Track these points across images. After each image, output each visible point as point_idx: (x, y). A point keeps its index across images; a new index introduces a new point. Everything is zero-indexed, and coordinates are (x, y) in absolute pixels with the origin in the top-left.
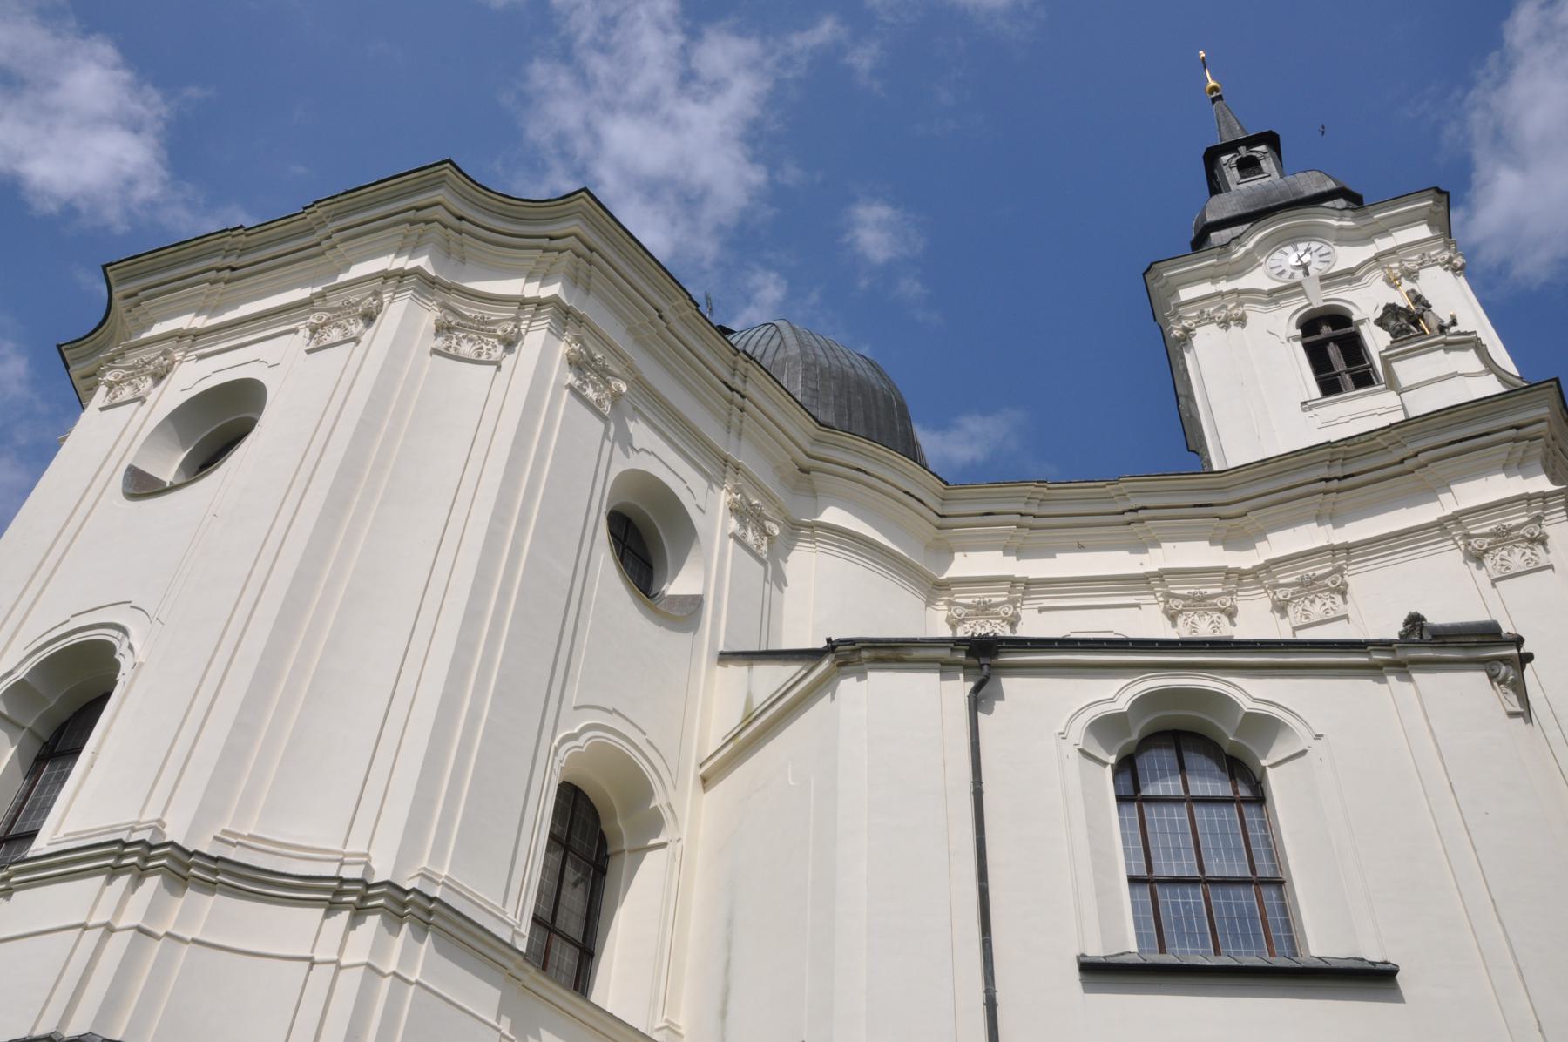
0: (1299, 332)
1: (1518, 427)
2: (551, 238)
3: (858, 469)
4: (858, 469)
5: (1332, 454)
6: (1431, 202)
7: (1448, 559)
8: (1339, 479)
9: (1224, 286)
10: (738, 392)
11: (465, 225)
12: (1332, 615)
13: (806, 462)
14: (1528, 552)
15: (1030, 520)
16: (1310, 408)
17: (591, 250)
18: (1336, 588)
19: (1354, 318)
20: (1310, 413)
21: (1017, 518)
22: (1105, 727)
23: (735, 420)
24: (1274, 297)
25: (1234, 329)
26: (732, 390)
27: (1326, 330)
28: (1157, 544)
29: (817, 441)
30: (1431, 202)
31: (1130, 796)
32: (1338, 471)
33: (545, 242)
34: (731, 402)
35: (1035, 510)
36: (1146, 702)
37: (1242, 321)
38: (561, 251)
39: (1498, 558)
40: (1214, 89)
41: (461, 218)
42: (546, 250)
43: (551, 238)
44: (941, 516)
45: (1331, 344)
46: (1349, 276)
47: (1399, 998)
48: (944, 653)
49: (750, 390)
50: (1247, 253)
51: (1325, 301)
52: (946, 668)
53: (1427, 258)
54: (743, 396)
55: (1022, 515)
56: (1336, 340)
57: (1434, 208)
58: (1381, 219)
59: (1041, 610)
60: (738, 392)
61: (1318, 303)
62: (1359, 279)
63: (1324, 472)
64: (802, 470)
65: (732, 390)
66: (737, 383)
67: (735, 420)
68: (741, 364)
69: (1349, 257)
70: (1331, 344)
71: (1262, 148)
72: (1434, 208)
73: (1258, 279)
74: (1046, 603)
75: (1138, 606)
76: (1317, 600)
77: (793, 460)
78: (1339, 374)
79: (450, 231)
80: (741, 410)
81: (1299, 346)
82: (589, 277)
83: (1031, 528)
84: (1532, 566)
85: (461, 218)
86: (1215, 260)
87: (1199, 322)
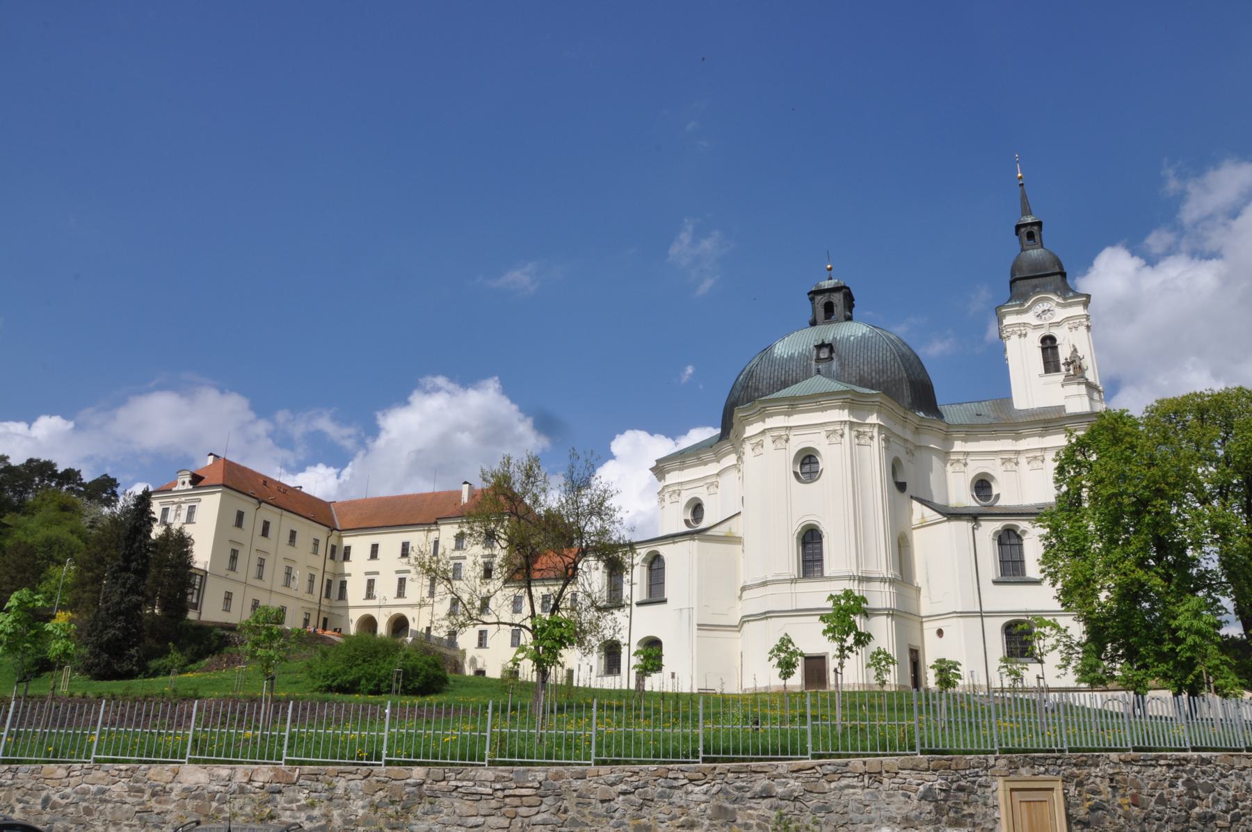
19: (1057, 343)
24: (1036, 327)
25: (1022, 338)
27: (1048, 342)
29: (920, 421)
31: (1000, 544)
36: (1004, 527)
37: (1025, 335)
40: (1021, 178)
46: (1058, 324)
49: (909, 417)
52: (968, 520)
61: (1047, 334)
64: (917, 428)
69: (1061, 314)
71: (1036, 228)
73: (1030, 318)
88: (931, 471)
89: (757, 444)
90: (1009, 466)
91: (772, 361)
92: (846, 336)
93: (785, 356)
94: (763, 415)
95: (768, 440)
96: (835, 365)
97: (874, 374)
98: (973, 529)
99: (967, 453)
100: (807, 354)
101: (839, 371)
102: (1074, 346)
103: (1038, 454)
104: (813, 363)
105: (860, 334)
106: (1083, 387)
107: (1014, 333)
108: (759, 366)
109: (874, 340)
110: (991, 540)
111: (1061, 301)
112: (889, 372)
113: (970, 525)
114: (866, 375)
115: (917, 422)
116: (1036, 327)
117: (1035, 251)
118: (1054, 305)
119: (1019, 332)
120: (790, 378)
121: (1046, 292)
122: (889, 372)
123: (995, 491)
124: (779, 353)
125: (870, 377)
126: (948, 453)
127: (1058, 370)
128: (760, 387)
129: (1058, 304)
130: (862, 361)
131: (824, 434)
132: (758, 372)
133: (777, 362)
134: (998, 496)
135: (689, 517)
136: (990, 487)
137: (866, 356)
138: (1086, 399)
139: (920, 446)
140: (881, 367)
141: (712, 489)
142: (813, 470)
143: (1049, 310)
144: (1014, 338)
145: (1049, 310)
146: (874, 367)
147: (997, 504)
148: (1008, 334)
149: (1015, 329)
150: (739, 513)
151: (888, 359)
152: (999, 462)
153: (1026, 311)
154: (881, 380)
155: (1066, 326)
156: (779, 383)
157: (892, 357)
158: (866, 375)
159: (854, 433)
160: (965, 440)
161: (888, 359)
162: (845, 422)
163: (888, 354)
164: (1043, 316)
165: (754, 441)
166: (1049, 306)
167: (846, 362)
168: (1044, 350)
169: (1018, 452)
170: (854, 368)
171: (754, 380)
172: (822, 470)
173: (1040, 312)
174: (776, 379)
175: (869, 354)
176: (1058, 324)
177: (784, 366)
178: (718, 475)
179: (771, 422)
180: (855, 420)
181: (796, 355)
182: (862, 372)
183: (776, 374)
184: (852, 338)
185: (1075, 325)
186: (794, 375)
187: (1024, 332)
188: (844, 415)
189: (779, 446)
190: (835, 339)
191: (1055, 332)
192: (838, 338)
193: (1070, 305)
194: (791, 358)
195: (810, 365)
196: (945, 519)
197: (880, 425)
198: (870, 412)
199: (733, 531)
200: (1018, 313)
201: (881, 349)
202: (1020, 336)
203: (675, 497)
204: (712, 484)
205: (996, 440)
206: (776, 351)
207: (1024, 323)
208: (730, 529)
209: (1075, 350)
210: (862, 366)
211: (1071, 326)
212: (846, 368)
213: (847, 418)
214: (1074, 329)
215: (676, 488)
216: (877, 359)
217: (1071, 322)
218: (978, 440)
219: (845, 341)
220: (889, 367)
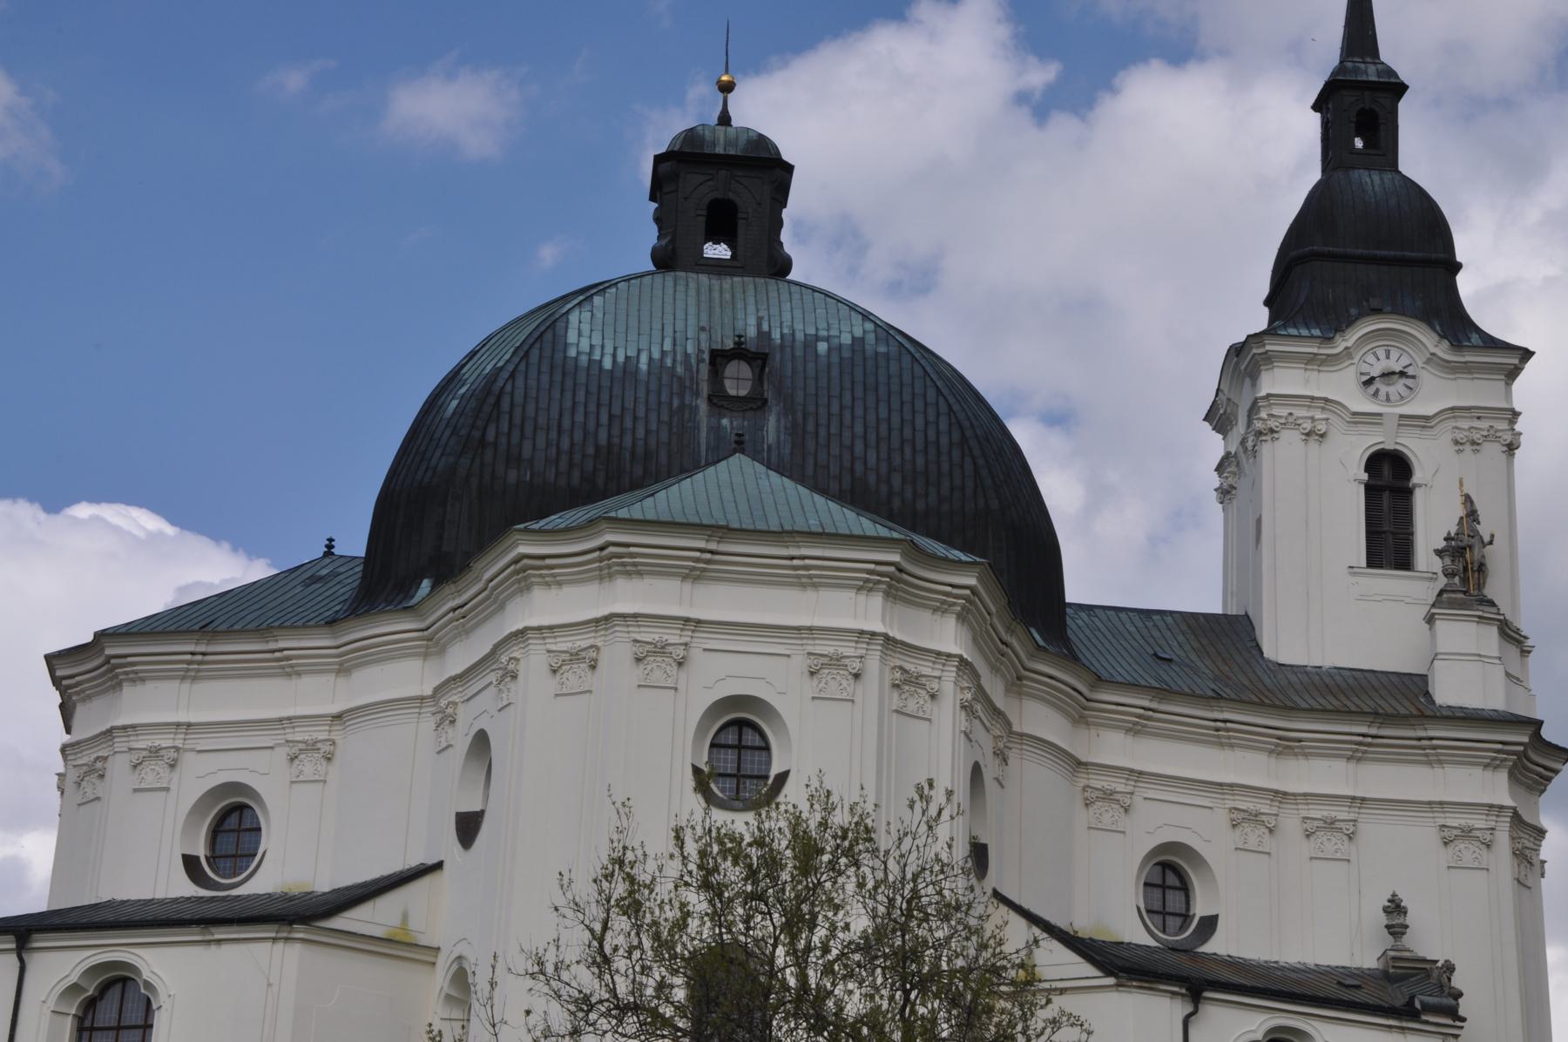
0: (1365, 477)
7: (1424, 833)
12: (1338, 856)
14: (1478, 851)
16: (1355, 574)
18: (1348, 835)
19: (1417, 477)
20: (1354, 579)
25: (1313, 443)
27: (1386, 470)
32: (1373, 731)
39: (1457, 848)
44: (1088, 700)
45: (1387, 492)
46: (1423, 422)
50: (1347, 348)
51: (1396, 443)
53: (1492, 432)
56: (1393, 490)
61: (1389, 446)
64: (1019, 678)
70: (1387, 492)
74: (1150, 794)
76: (1333, 839)
78: (1384, 532)
81: (1362, 488)
84: (1476, 865)
87: (1285, 424)
89: (575, 656)
90: (1254, 836)
91: (566, 371)
92: (800, 336)
93: (607, 364)
94: (611, 565)
95: (617, 650)
96: (772, 426)
97: (896, 480)
100: (679, 370)
101: (787, 451)
102: (1468, 500)
103: (1342, 813)
104: (703, 406)
105: (846, 339)
106: (1493, 631)
107: (1292, 423)
108: (520, 382)
109: (894, 368)
111: (1442, 350)
112: (946, 485)
113: (1180, 1008)
114: (872, 478)
116: (1360, 418)
117: (1376, 178)
119: (1308, 426)
120: (628, 441)
121: (1399, 311)
122: (946, 485)
123: (1200, 909)
124: (585, 345)
125: (884, 489)
127: (1403, 560)
128: (527, 451)
129: (1432, 359)
130: (859, 429)
131: (800, 663)
132: (519, 398)
133: (582, 378)
134: (1209, 925)
135: (201, 850)
136: (1185, 888)
137: (871, 417)
138: (1498, 672)
140: (920, 461)
141: (309, 766)
142: (748, 769)
143: (1402, 374)
144: (1290, 440)
145: (1402, 374)
146: (897, 461)
147: (1208, 948)
148: (1272, 424)
149: (1300, 413)
150: (438, 866)
151: (944, 441)
154: (920, 505)
156: (591, 450)
157: (956, 436)
158: (872, 478)
160: (1135, 730)
161: (944, 441)
162: (873, 634)
163: (943, 426)
164: (1384, 389)
165: (564, 644)
166: (1405, 361)
167: (810, 427)
168: (1371, 491)
169: (1281, 796)
170: (835, 450)
171: (505, 427)
172: (782, 778)
173: (1375, 372)
174: (578, 436)
175: (883, 413)
177: (605, 397)
178: (338, 717)
179: (627, 596)
181: (643, 366)
182: (859, 467)
183: (579, 418)
184: (822, 347)
185: (1476, 436)
186: (641, 433)
187: (1322, 427)
188: (870, 613)
189: (657, 677)
190: (764, 336)
191: (1415, 447)
192: (776, 335)
193: (1467, 369)
194: (627, 370)
195: (694, 410)
196: (1111, 981)
197: (961, 658)
199: (414, 924)
200: (1311, 360)
201: (919, 405)
203: (153, 774)
204: (312, 746)
206: (572, 337)
207: (1326, 400)
208: (405, 917)
209: (1472, 515)
210: (859, 448)
211: (1460, 436)
212: (811, 445)
213: (878, 627)
214: (1468, 448)
215: (164, 741)
216: (908, 433)
217: (1465, 424)
219: (799, 353)
220: (945, 467)
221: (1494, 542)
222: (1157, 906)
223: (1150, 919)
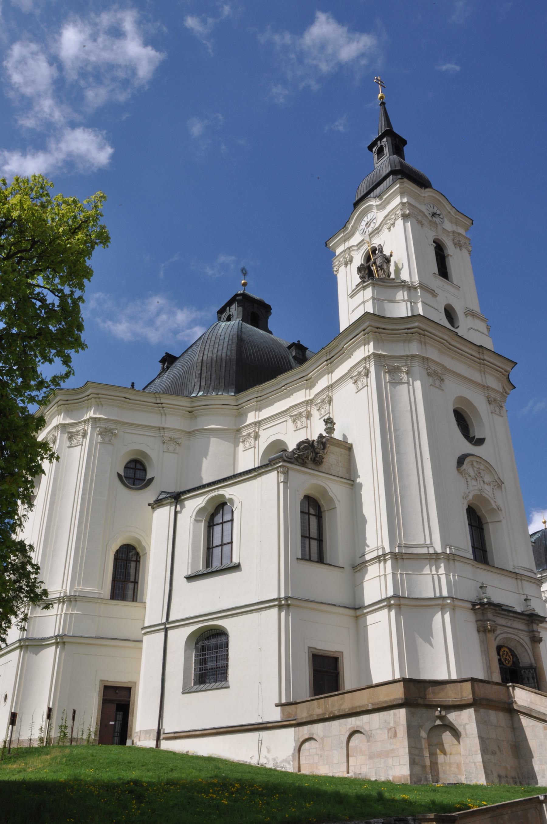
1: (364, 330)
2: (88, 396)
3: (205, 405)
4: (205, 405)
5: (326, 351)
6: (398, 185)
8: (330, 359)
9: (347, 245)
10: (159, 403)
11: (69, 402)
13: (190, 409)
15: (259, 399)
17: (98, 394)
21: (255, 399)
22: (201, 511)
23: (162, 412)
25: (349, 266)
26: (158, 404)
28: (292, 394)
30: (398, 185)
32: (328, 357)
33: (86, 398)
34: (159, 407)
35: (259, 395)
38: (91, 399)
41: (67, 400)
42: (88, 400)
43: (88, 396)
47: (241, 570)
48: (169, 501)
49: (163, 401)
50: (352, 226)
54: (162, 404)
55: (257, 398)
57: (402, 186)
58: (386, 198)
59: (264, 430)
60: (159, 403)
62: (381, 231)
63: (325, 359)
65: (158, 404)
66: (158, 401)
67: (162, 412)
68: (157, 396)
72: (402, 186)
74: (265, 427)
75: (286, 421)
77: (186, 411)
79: (66, 406)
80: (163, 408)
82: (101, 402)
83: (260, 401)
85: (67, 400)
86: (342, 235)
88: (206, 454)
98: (176, 513)
99: (258, 424)
110: (192, 521)
115: (189, 405)
118: (375, 210)
126: (239, 431)
139: (194, 431)
152: (290, 421)
153: (352, 234)
155: (385, 230)
159: (66, 436)
176: (377, 231)
180: (68, 421)
193: (388, 202)
198: (89, 408)
202: (346, 265)
205: (289, 396)
218: (272, 404)
221: (393, 255)
222: (132, 475)
223: (126, 481)
